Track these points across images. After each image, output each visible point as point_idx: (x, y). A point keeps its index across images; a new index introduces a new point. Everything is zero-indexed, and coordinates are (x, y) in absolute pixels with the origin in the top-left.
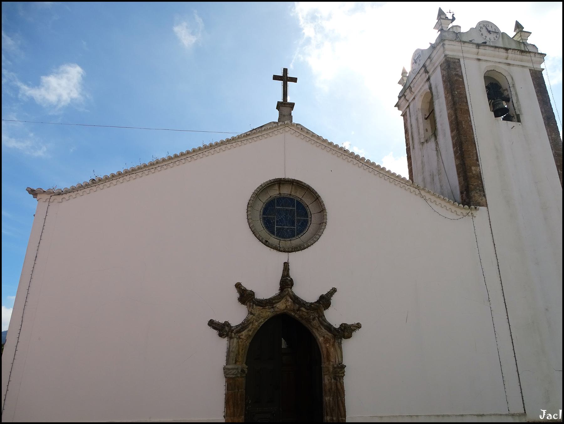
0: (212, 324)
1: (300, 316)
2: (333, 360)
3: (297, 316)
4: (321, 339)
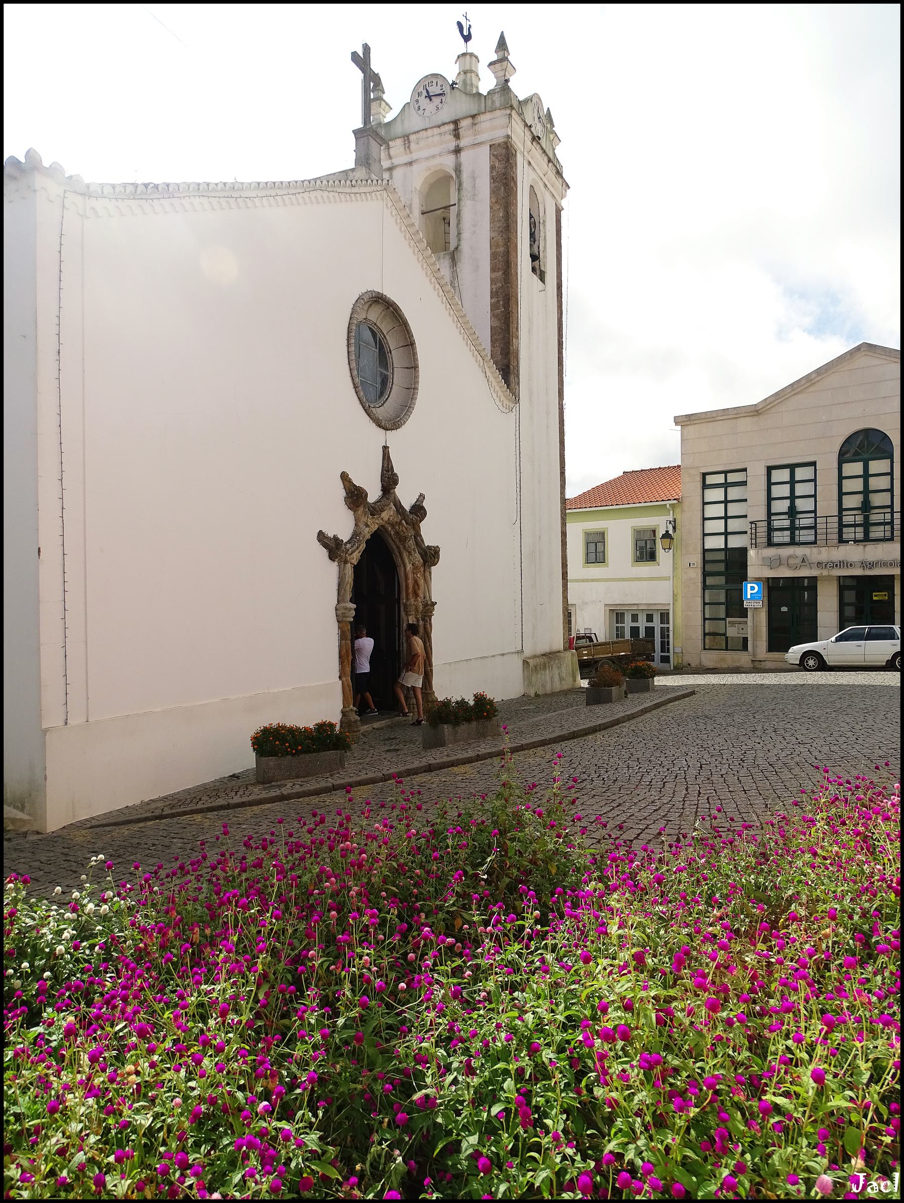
0: (321, 537)
1: (397, 533)
2: (422, 596)
3: (392, 533)
4: (409, 567)
